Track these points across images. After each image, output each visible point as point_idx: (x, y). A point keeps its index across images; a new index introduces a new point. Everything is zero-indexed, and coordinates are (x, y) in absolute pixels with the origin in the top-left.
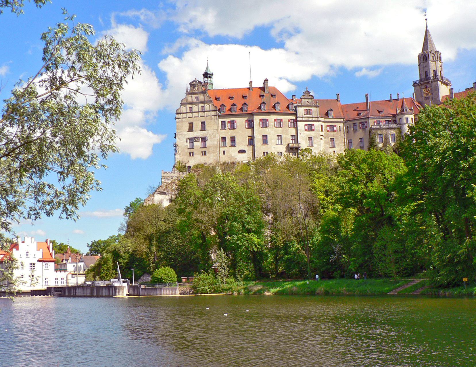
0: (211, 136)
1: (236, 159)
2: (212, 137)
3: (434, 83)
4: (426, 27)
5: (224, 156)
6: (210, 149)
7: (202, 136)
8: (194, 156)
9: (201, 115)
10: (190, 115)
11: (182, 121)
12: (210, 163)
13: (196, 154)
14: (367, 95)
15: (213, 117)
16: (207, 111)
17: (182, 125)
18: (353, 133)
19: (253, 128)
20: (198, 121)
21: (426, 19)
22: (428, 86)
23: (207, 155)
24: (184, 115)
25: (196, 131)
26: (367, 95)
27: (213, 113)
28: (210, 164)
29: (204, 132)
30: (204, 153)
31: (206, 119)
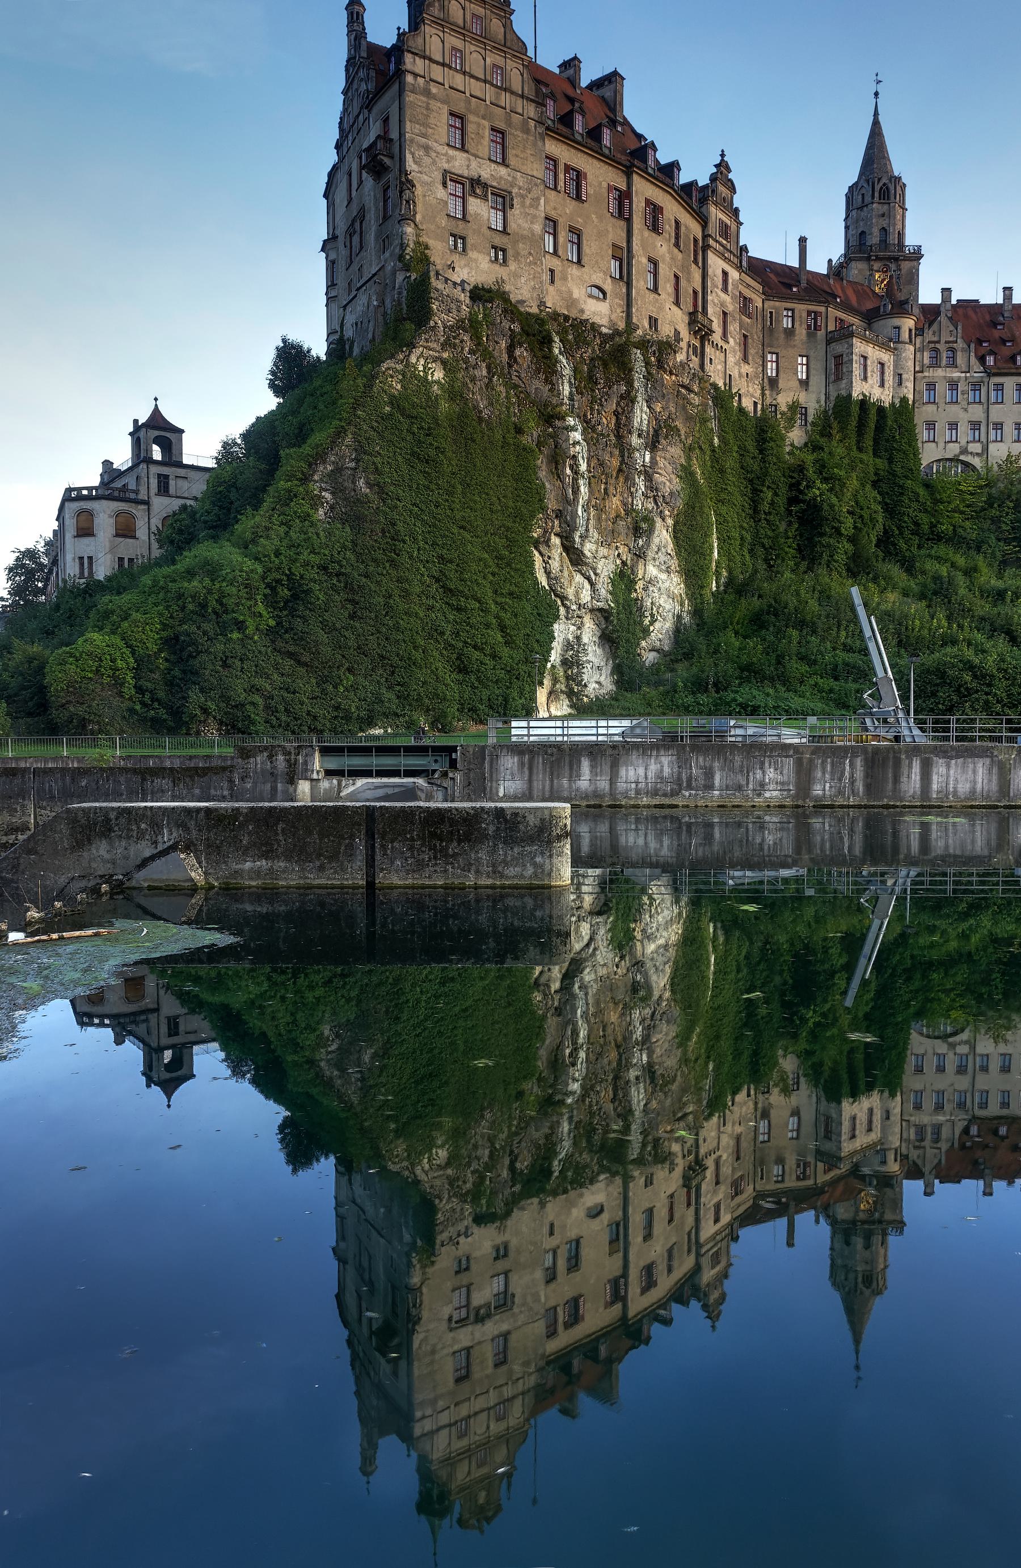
0: (523, 197)
1: (582, 311)
2: (528, 202)
3: (905, 265)
4: (876, 114)
5: (551, 288)
6: (521, 245)
7: (495, 184)
8: (473, 254)
9: (493, 101)
10: (459, 80)
11: (427, 93)
12: (520, 298)
13: (475, 247)
14: (803, 241)
15: (532, 123)
16: (512, 93)
17: (428, 109)
18: (782, 336)
19: (629, 221)
20: (484, 118)
21: (876, 94)
22: (893, 266)
23: (513, 266)
24: (437, 73)
25: (476, 156)
26: (803, 241)
27: (531, 110)
28: (522, 302)
29: (503, 171)
30: (501, 254)
31: (509, 123)
